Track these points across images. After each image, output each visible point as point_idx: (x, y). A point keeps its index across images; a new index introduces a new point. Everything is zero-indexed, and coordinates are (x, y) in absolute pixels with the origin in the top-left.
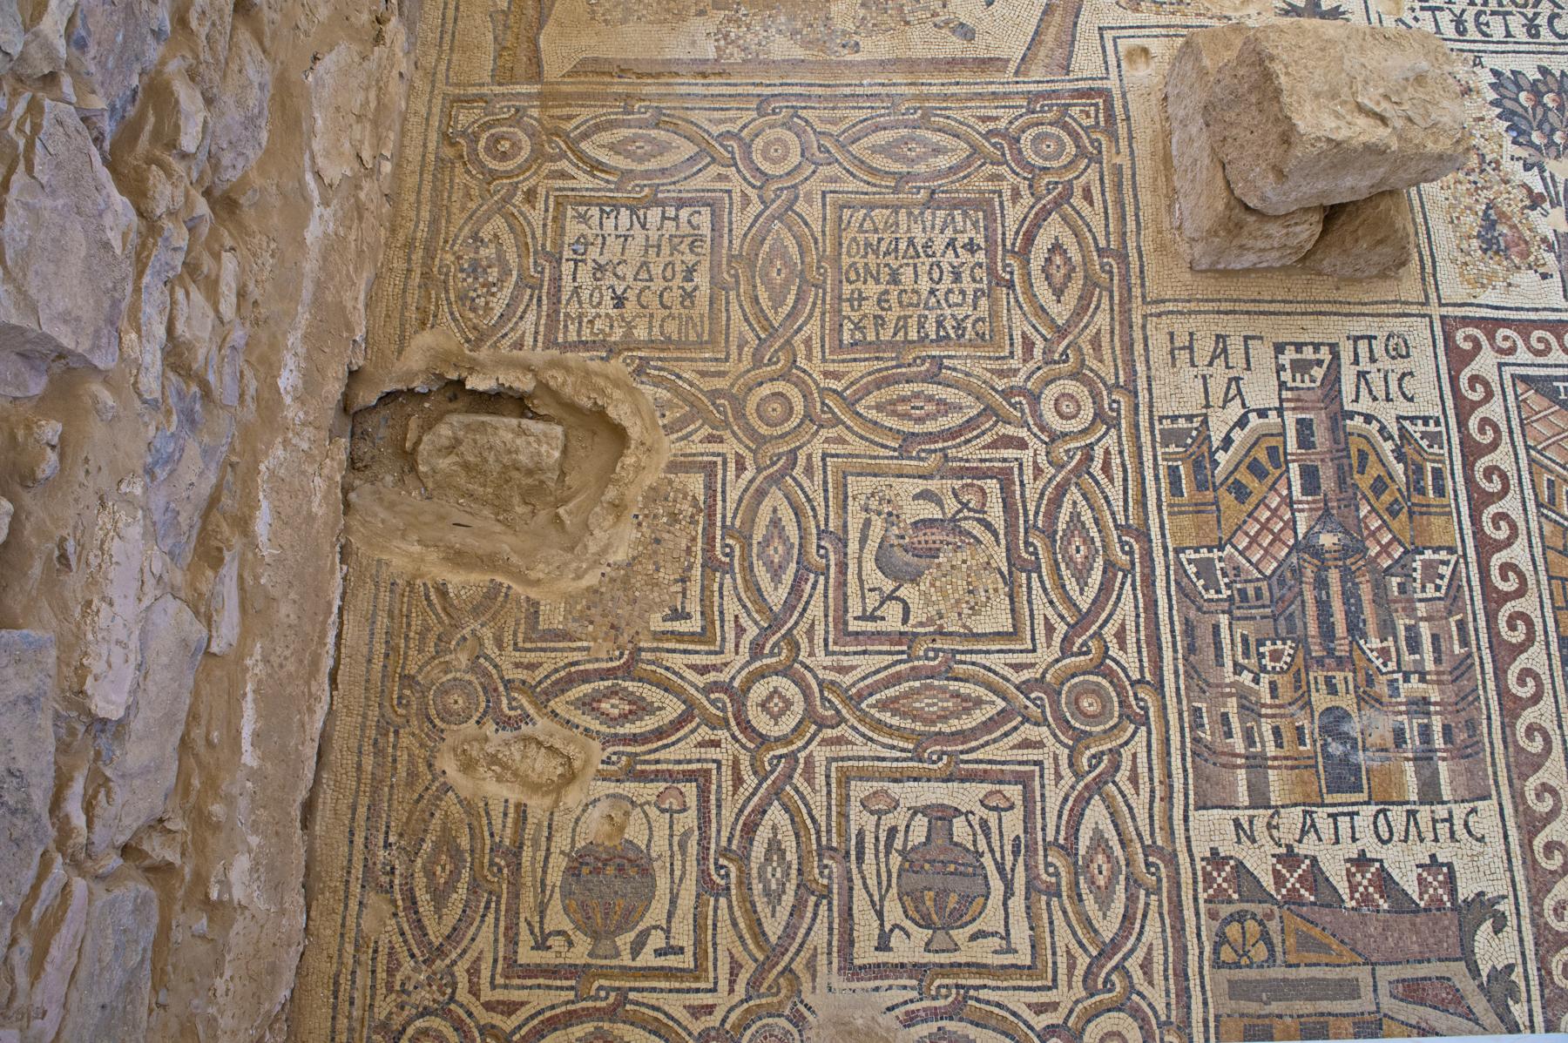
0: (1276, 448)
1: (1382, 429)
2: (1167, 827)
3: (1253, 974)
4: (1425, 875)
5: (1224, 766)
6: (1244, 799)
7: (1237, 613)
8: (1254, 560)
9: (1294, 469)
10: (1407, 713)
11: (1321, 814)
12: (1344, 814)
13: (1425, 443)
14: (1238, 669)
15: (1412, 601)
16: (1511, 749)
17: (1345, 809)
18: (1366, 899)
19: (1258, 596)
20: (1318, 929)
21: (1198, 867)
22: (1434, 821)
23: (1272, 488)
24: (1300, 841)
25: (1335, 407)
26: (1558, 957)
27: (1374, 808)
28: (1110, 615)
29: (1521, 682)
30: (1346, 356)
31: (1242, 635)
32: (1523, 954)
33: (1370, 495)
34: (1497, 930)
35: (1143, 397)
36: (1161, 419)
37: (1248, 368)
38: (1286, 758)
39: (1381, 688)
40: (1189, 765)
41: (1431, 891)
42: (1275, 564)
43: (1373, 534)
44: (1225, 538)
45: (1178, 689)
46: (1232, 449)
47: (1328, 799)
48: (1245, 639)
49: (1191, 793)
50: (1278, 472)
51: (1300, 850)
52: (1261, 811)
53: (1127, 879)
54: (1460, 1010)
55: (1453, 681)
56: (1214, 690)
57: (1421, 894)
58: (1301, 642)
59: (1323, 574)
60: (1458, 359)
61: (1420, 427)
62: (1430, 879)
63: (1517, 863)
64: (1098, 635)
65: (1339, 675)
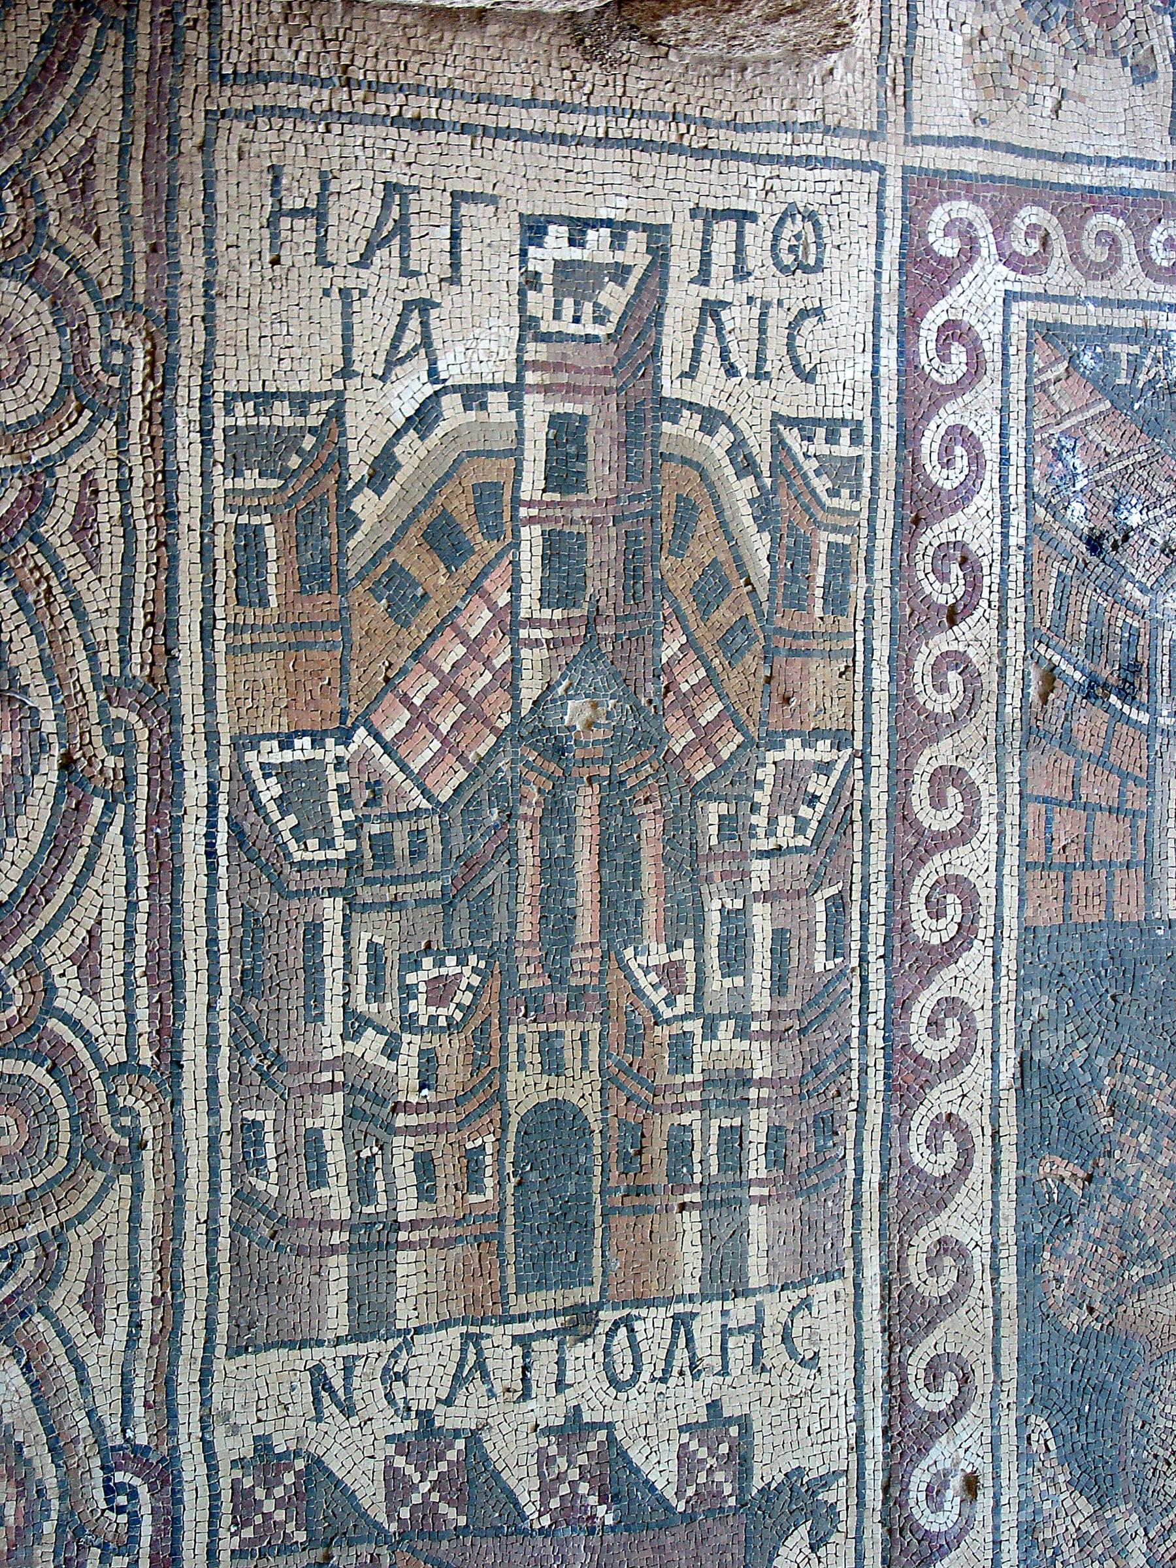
1: (737, 447)
6: (337, 1320)
10: (704, 1105)
11: (499, 1337)
12: (547, 1334)
13: (821, 485)
15: (743, 856)
19: (417, 853)
21: (225, 1484)
22: (725, 1331)
24: (448, 1402)
28: (65, 909)
30: (682, 262)
35: (191, 338)
36: (231, 398)
37: (455, 280)
40: (223, 1257)
41: (702, 1479)
45: (213, 1082)
46: (393, 488)
47: (519, 1305)
49: (223, 1318)
50: (496, 547)
51: (447, 1419)
53: (60, 1527)
58: (500, 959)
60: (924, 276)
61: (820, 446)
64: (31, 959)
65: (570, 1029)
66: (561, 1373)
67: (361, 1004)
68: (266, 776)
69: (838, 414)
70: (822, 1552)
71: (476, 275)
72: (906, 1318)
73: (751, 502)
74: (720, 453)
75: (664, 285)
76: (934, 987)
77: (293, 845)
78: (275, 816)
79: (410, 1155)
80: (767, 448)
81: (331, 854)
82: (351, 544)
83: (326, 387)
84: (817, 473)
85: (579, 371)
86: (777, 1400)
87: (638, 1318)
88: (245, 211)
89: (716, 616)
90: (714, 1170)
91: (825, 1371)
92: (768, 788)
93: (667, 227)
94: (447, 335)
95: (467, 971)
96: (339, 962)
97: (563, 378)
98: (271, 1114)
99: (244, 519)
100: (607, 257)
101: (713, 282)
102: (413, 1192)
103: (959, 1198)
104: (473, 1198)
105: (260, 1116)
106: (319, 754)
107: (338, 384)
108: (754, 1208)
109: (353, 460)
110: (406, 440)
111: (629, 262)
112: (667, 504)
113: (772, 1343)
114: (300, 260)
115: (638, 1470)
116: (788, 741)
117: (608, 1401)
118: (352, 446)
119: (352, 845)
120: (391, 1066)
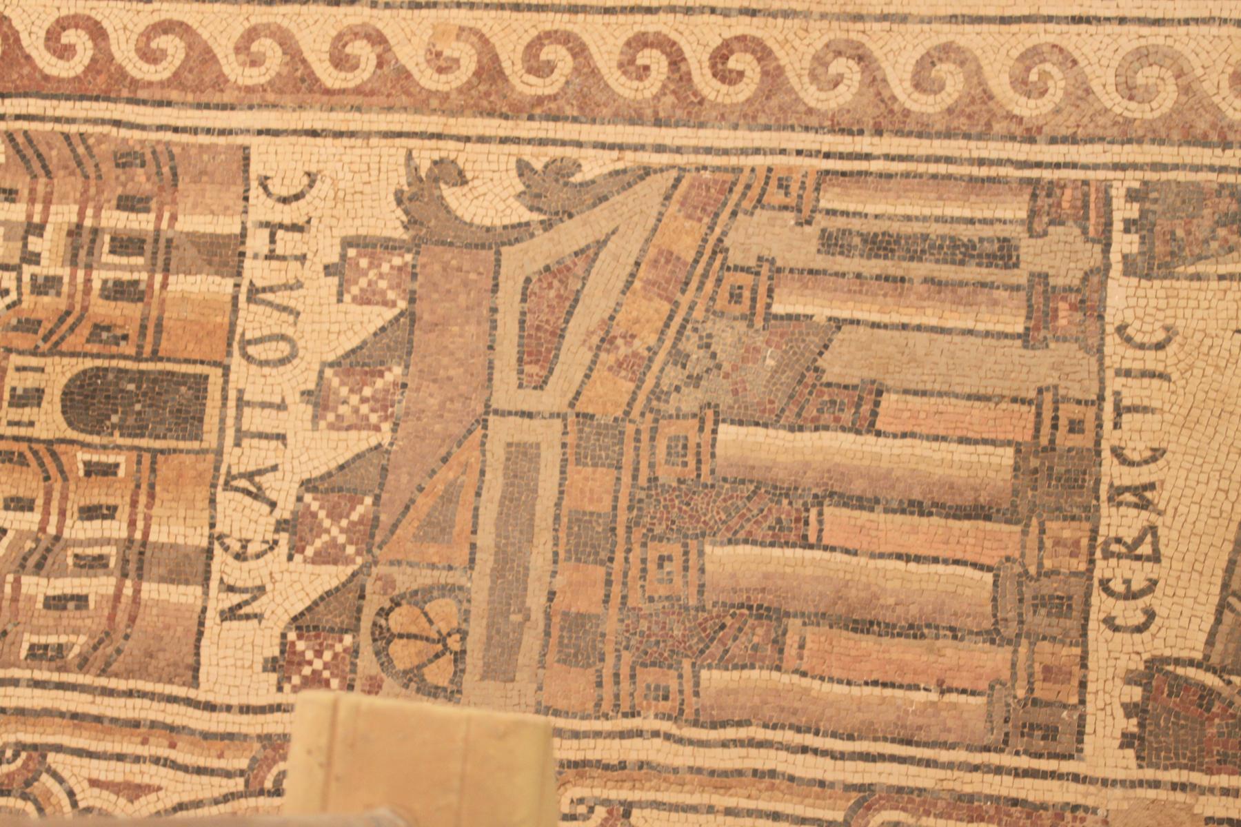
2: (219, 745)
3: (477, 630)
4: (355, 290)
5: (132, 619)
6: (187, 595)
10: (89, 267)
12: (239, 418)
16: (174, 95)
17: (231, 412)
18: (382, 404)
20: (421, 499)
22: (271, 256)
24: (273, 505)
26: (514, 80)
27: (236, 361)
29: (65, 52)
32: (504, 141)
34: (461, 179)
38: (134, 504)
41: (383, 284)
47: (210, 440)
52: (215, 566)
54: (579, 270)
55: (48, 173)
57: (385, 303)
62: (363, 282)
63: (356, 121)
66: (270, 405)
70: (469, 175)
72: (299, 84)
76: (34, 54)
79: (79, 524)
86: (335, 212)
87: (243, 335)
90: (140, 261)
91: (321, 166)
102: (107, 523)
103: (205, 36)
104: (121, 473)
105: (25, 646)
108: (179, 226)
113: (287, 214)
115: (365, 343)
117: (303, 365)
120: (10, 534)
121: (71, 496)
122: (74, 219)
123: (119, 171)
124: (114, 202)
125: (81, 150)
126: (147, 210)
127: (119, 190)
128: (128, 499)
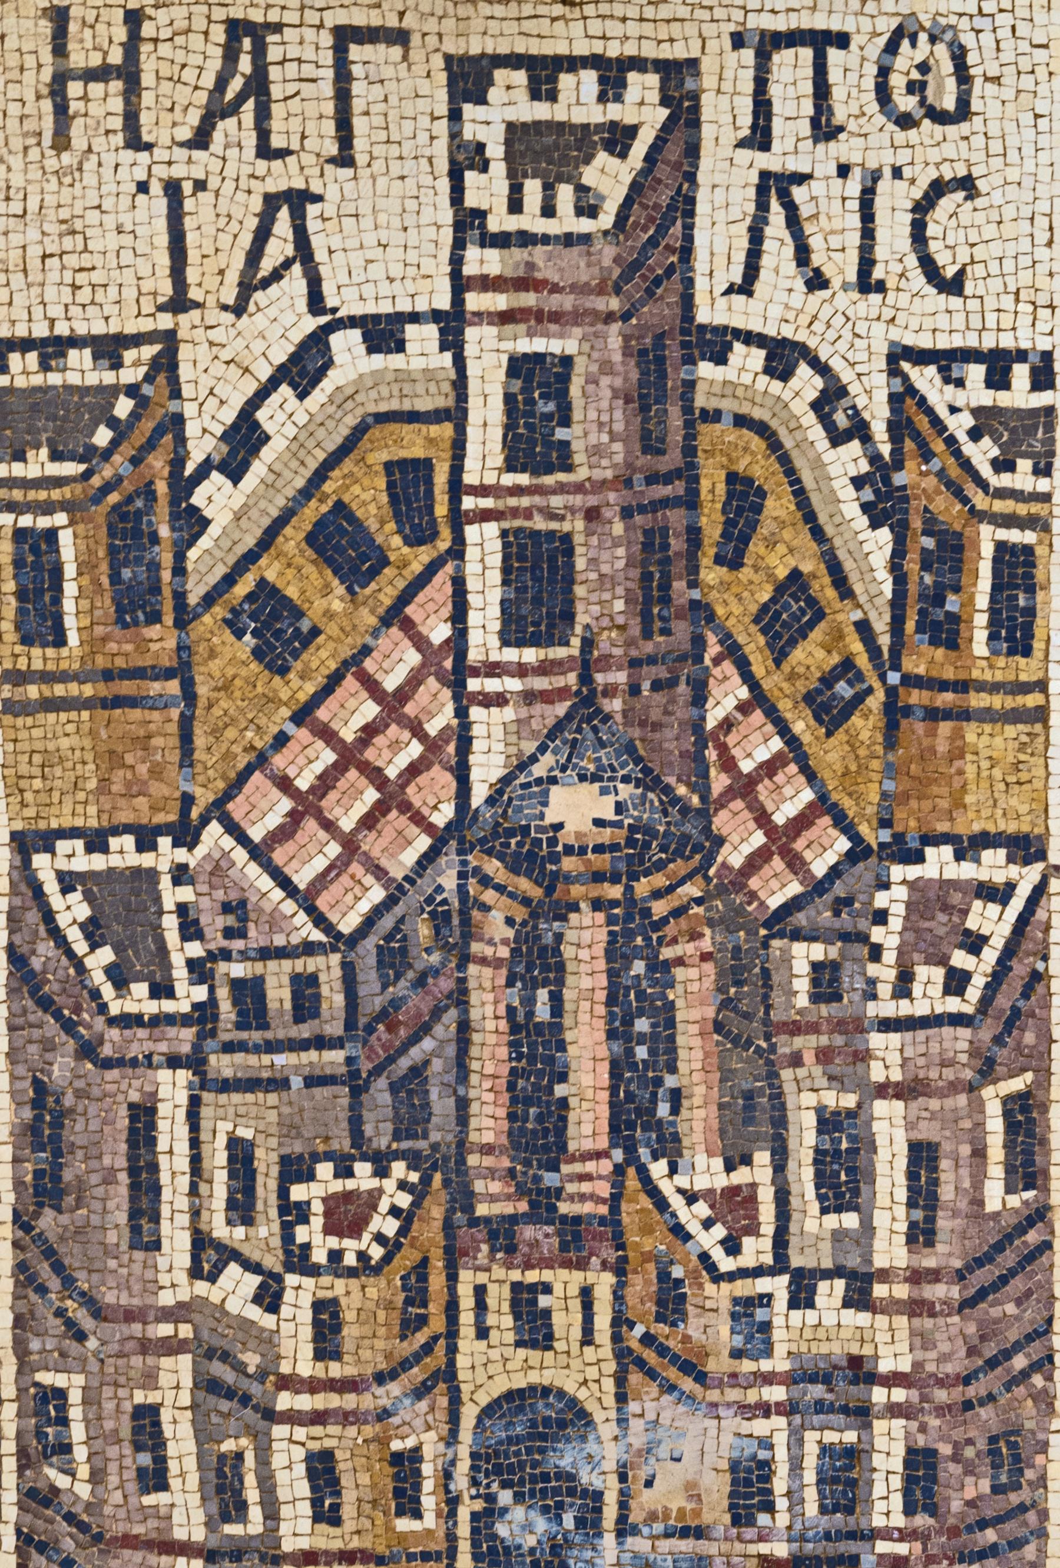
0: (424, 467)
1: (833, 393)
7: (222, 1065)
8: (302, 879)
9: (484, 543)
10: (789, 1409)
13: (982, 454)
14: (208, 1257)
15: (857, 1026)
23: (394, 615)
25: (661, 312)
30: (724, 114)
31: (234, 1143)
33: (754, 645)
37: (345, 159)
39: (710, 1327)
42: (377, 894)
43: (745, 787)
44: (204, 798)
46: (257, 470)
48: (241, 1156)
50: (424, 555)
56: (118, 1331)
58: (445, 1169)
59: (548, 930)
61: (976, 390)
65: (565, 1282)
67: (220, 1229)
68: (65, 890)
69: (1007, 342)
71: (378, 150)
73: (858, 482)
74: (801, 408)
75: (693, 151)
77: (108, 991)
78: (80, 947)
79: (299, 1453)
80: (881, 396)
81: (168, 1006)
82: (193, 554)
83: (146, 325)
84: (975, 435)
85: (555, 289)
88: (15, 75)
89: (798, 654)
90: (811, 1509)
92: (896, 923)
93: (693, 64)
94: (336, 243)
95: (389, 1185)
96: (183, 1164)
97: (529, 299)
98: (79, 1380)
99: (26, 521)
100: (592, 113)
101: (776, 145)
102: (305, 1508)
104: (404, 1524)
105: (60, 1380)
106: (147, 860)
107: (165, 321)
109: (192, 429)
110: (275, 399)
111: (630, 120)
112: (712, 484)
114: (99, 143)
116: (930, 852)
118: (189, 410)
119: (200, 993)
120: (268, 1321)
121: (352, 1431)
122: (884, 1366)
123: (982, 1445)
124: (921, 1441)
125: (1019, 1362)
126: (909, 1510)
127: (945, 1449)
128: (355, 1543)
